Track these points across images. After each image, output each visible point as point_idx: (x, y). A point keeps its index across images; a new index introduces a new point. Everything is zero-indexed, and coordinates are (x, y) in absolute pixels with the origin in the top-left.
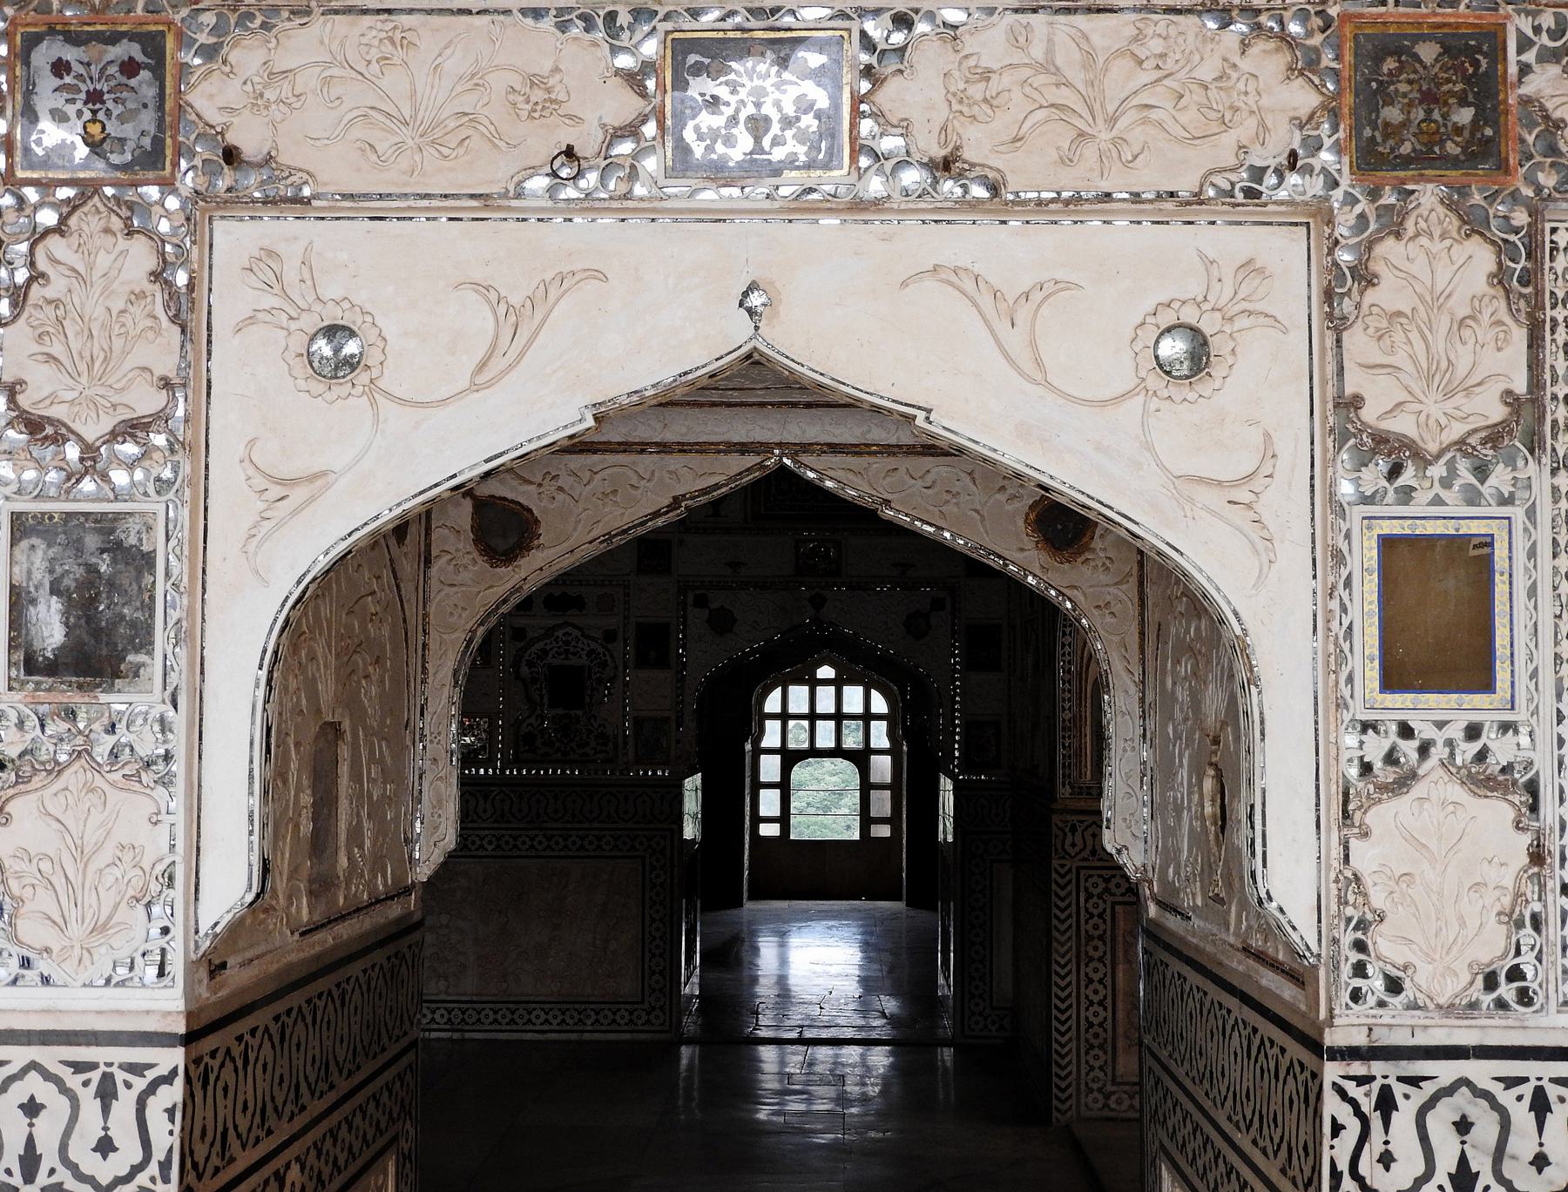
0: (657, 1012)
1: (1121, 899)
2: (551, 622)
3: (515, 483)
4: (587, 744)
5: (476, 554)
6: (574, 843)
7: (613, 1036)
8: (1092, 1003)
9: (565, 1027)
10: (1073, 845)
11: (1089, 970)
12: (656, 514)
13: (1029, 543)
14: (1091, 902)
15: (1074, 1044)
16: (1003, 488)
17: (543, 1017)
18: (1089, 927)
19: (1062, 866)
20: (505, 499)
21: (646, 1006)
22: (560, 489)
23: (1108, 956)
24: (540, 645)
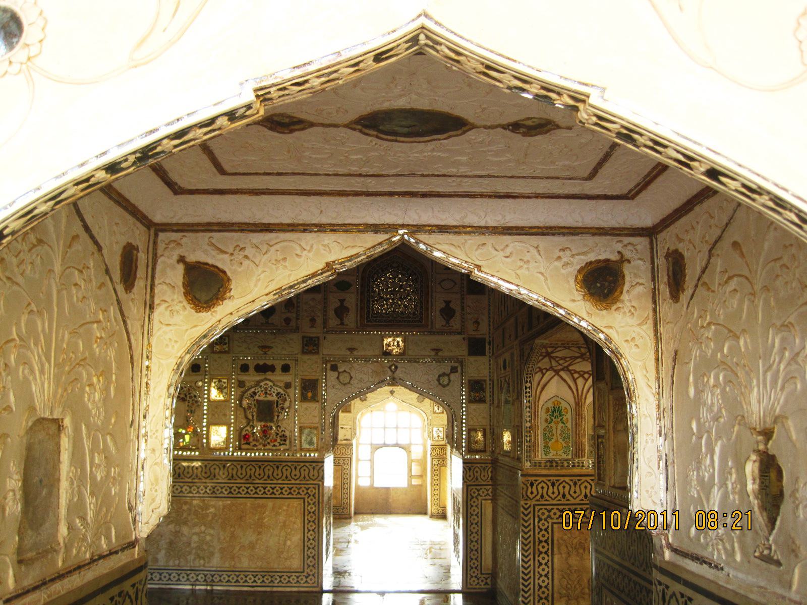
0: (311, 577)
1: (556, 521)
2: (258, 378)
3: (214, 253)
4: (275, 440)
5: (185, 303)
6: (269, 491)
7: (288, 589)
8: (541, 576)
9: (263, 584)
10: (532, 493)
11: (540, 559)
12: (314, 275)
13: (578, 296)
14: (541, 522)
15: (531, 598)
16: (559, 258)
17: (253, 579)
18: (540, 536)
19: (526, 504)
20: (207, 264)
21: (305, 574)
22: (246, 257)
23: (550, 551)
24: (253, 390)
